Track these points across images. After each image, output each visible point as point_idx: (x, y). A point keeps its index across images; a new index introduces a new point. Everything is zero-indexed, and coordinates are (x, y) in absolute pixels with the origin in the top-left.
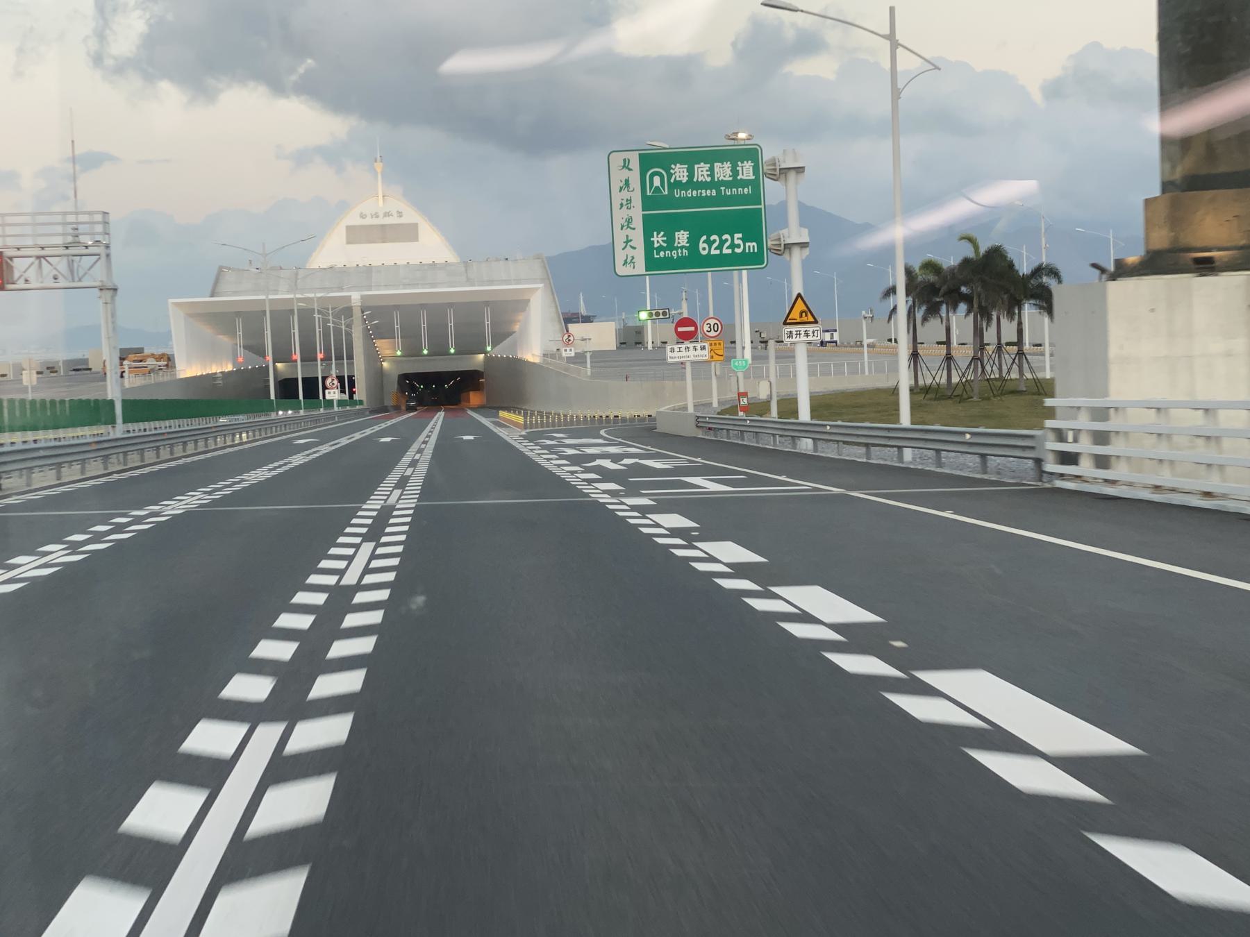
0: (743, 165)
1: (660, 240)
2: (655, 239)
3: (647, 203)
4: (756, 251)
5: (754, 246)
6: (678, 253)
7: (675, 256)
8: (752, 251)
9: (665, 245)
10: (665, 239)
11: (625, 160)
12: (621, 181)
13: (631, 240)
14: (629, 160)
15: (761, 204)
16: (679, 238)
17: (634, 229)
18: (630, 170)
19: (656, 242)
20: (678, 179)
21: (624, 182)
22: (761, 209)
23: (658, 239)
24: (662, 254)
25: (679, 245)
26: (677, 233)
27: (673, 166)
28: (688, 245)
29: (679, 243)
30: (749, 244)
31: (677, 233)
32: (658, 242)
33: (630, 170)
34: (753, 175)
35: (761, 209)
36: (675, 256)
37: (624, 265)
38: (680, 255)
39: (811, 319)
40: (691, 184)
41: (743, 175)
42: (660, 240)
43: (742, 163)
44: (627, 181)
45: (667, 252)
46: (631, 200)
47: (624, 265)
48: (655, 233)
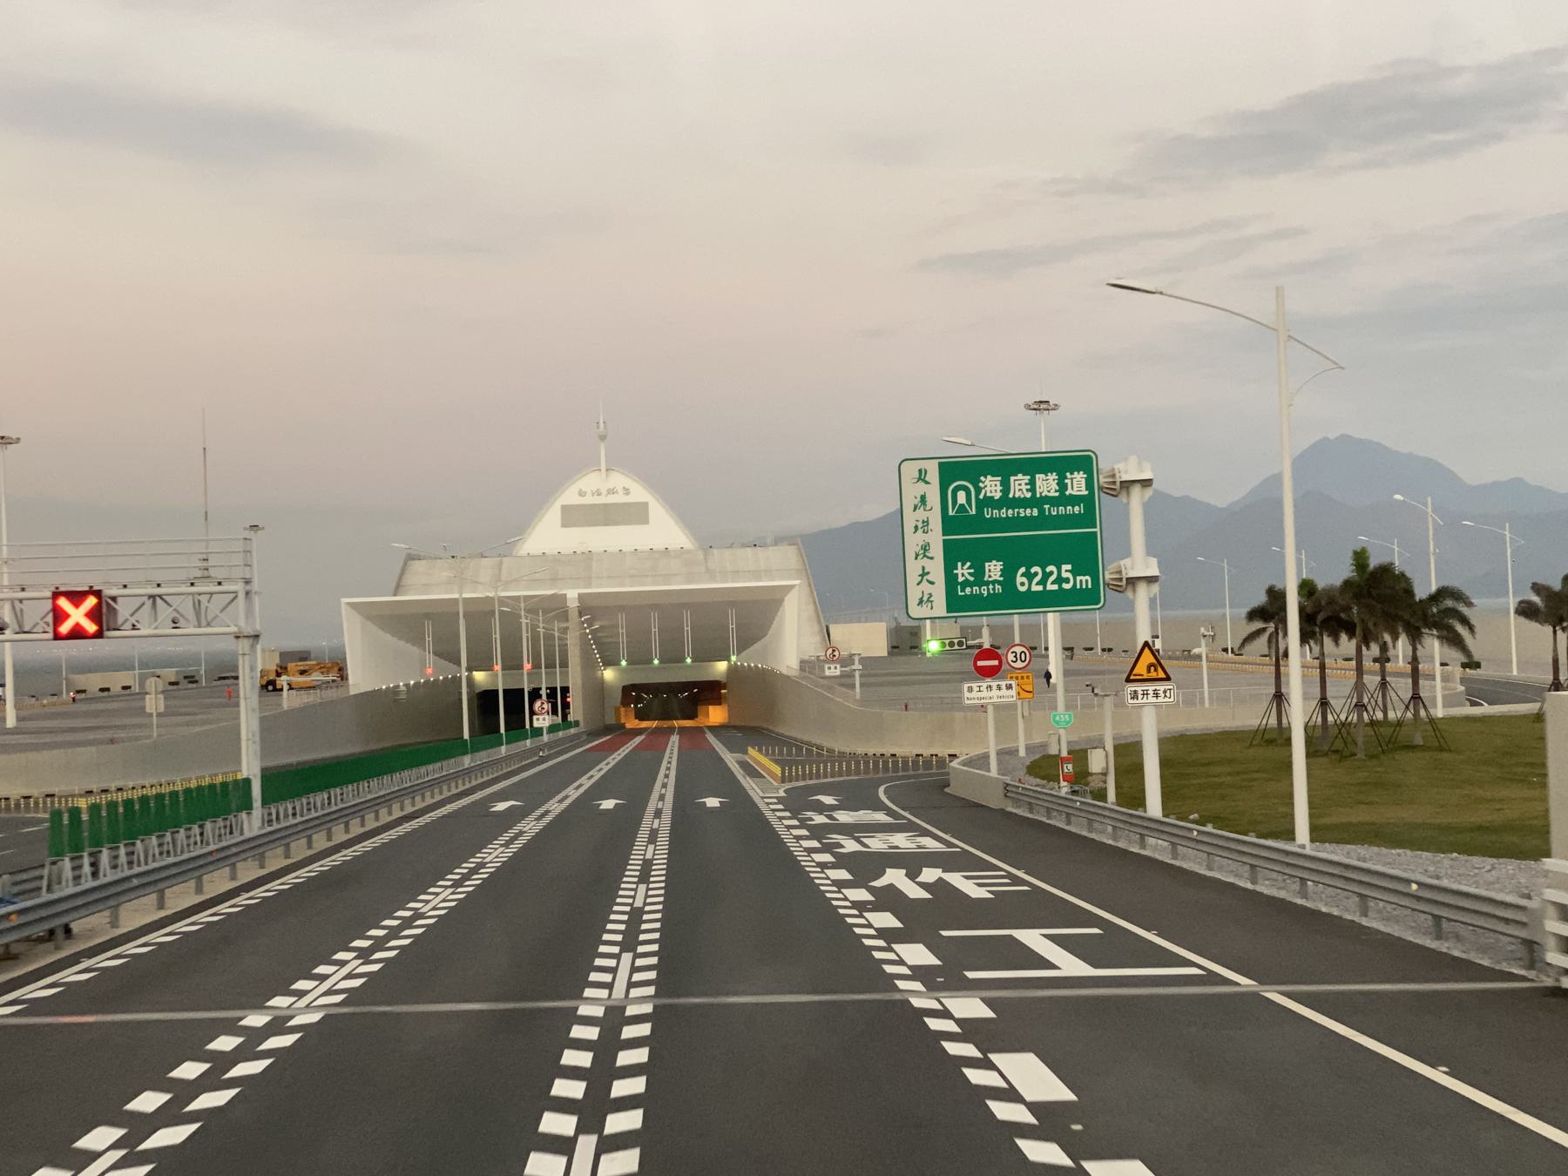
0: (1073, 476)
1: (965, 572)
2: (959, 571)
3: (949, 525)
4: (1090, 587)
5: (1087, 581)
6: (988, 589)
7: (985, 593)
8: (1084, 587)
9: (972, 579)
10: (972, 571)
11: (920, 471)
13: (928, 573)
15: (1096, 527)
16: (990, 571)
17: (932, 558)
18: (927, 483)
19: (960, 575)
20: (989, 494)
21: (919, 499)
22: (1096, 533)
23: (963, 572)
24: (968, 590)
25: (990, 579)
26: (987, 564)
27: (982, 478)
28: (1002, 579)
29: (990, 576)
30: (1082, 577)
31: (987, 564)
32: (963, 575)
33: (927, 483)
34: (1086, 490)
35: (1096, 533)
36: (985, 593)
37: (918, 605)
38: (992, 592)
39: (1162, 675)
40: (1006, 501)
42: (965, 572)
43: (1072, 474)
44: (923, 498)
45: (974, 588)
46: (928, 522)
47: (918, 605)
48: (959, 564)
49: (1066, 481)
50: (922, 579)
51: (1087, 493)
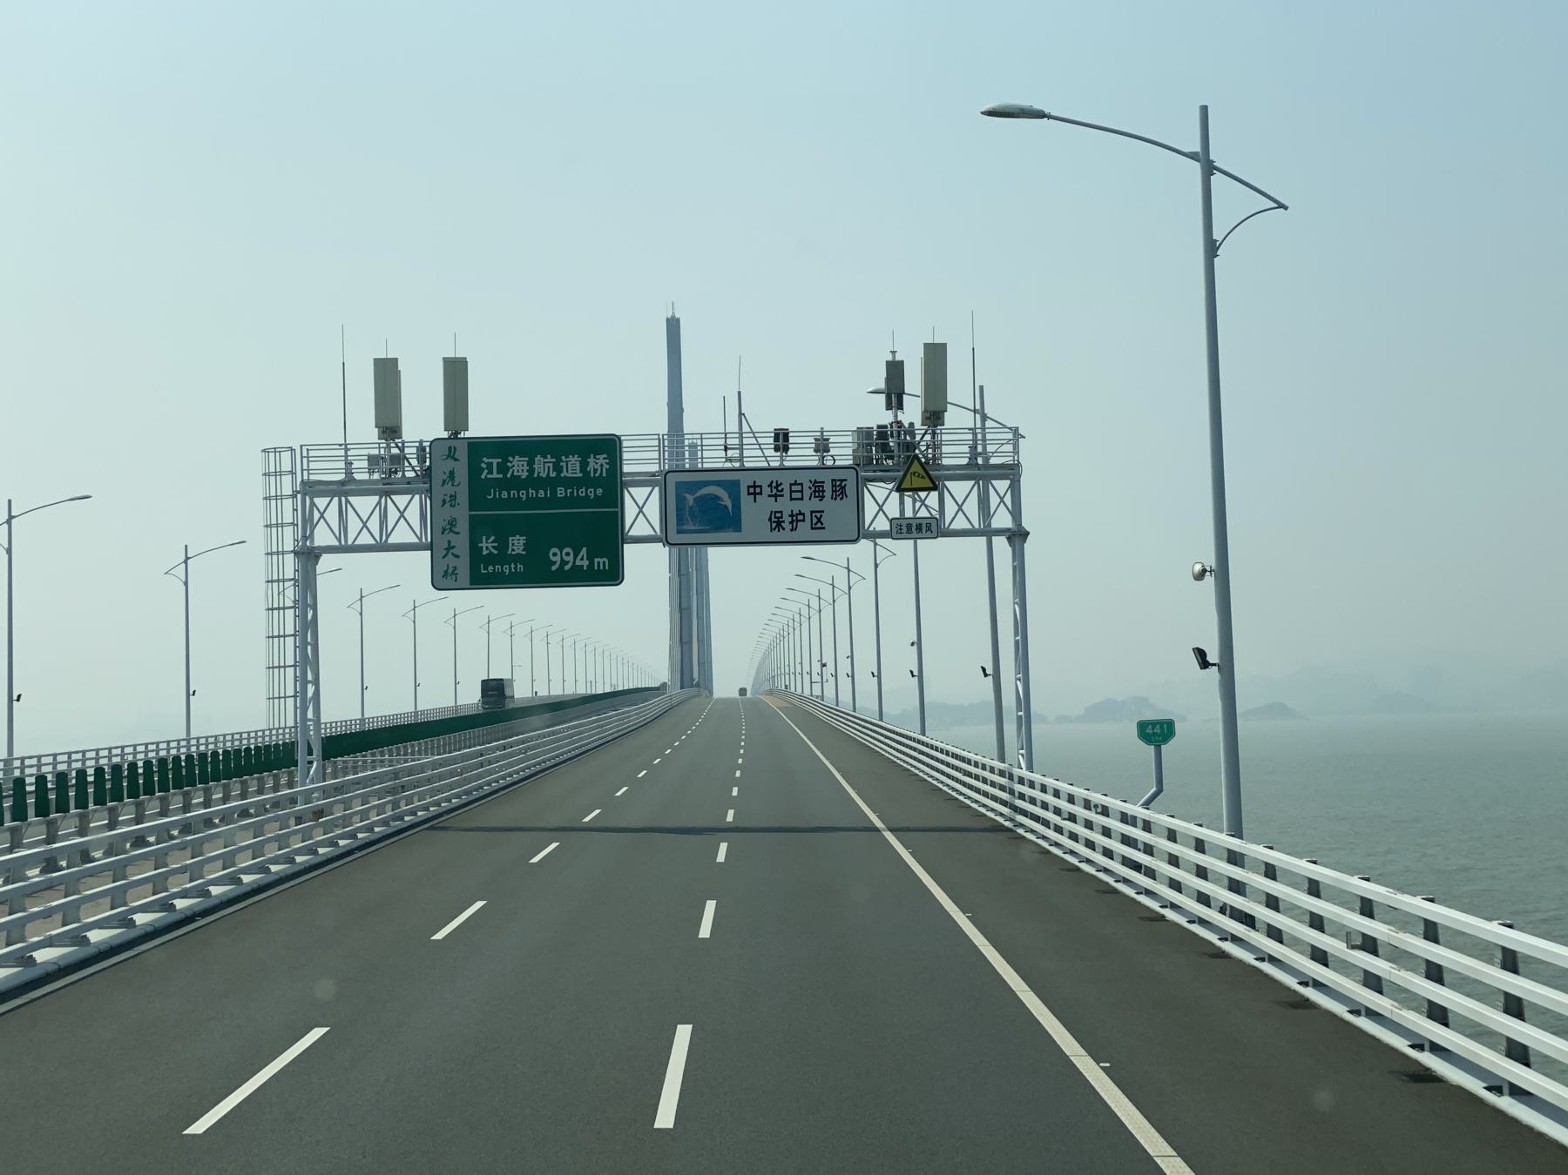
1: (489, 545)
2: (484, 545)
4: (607, 568)
5: (604, 562)
8: (601, 568)
10: (496, 544)
11: (450, 448)
12: (445, 473)
13: (454, 547)
14: (455, 448)
16: (513, 545)
17: (458, 533)
18: (456, 460)
19: (484, 548)
20: (515, 474)
22: (617, 512)
24: (491, 568)
26: (511, 538)
28: (524, 553)
29: (513, 550)
30: (599, 559)
31: (511, 538)
32: (487, 548)
33: (456, 460)
35: (617, 512)
41: (567, 471)
46: (455, 496)
48: (484, 538)
49: (561, 464)
50: (448, 552)
51: (581, 475)
